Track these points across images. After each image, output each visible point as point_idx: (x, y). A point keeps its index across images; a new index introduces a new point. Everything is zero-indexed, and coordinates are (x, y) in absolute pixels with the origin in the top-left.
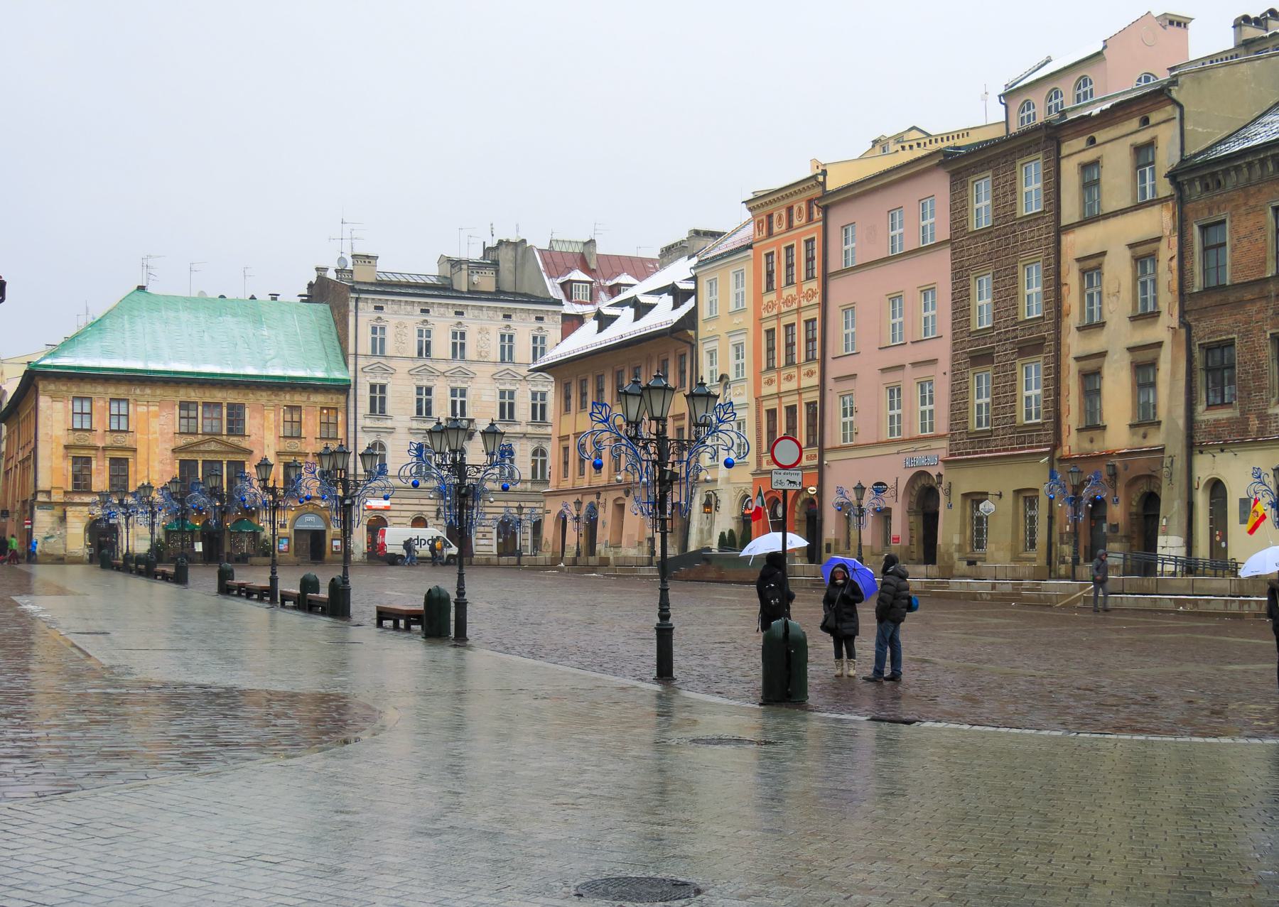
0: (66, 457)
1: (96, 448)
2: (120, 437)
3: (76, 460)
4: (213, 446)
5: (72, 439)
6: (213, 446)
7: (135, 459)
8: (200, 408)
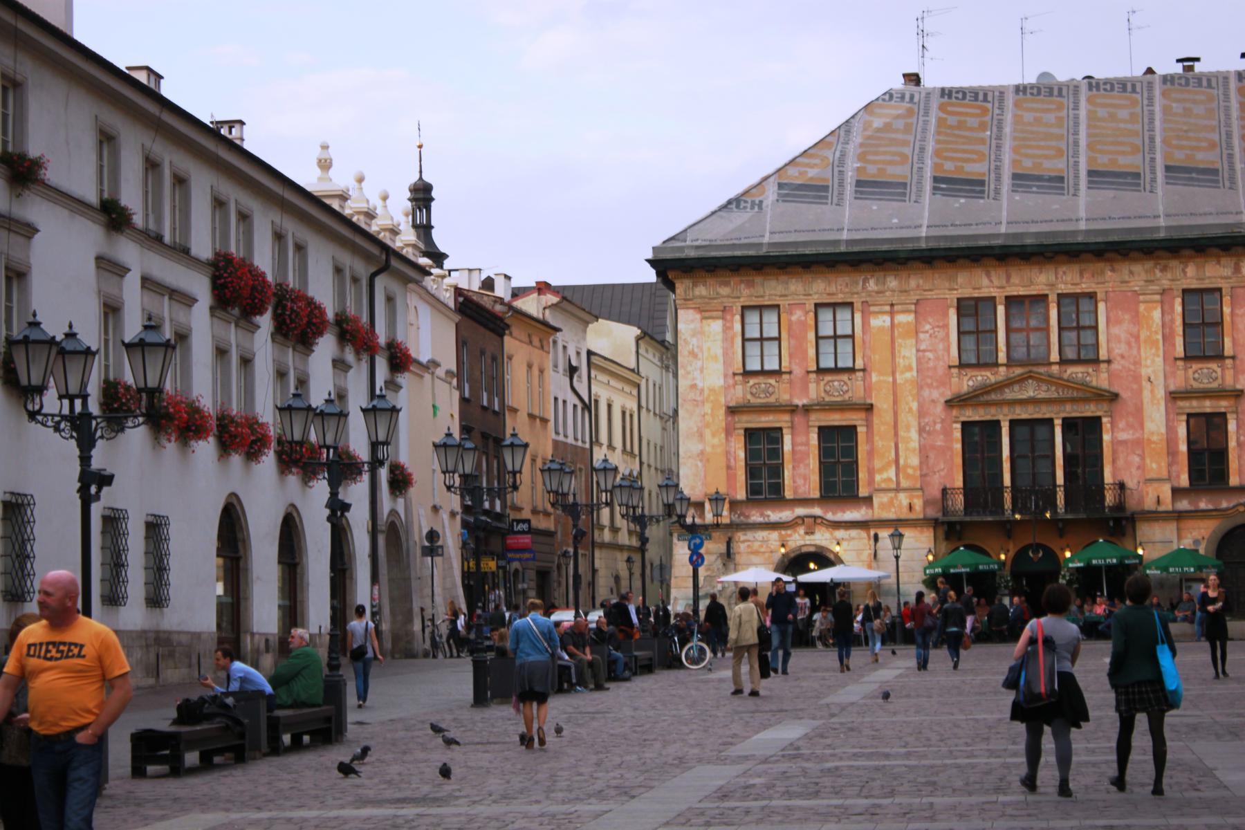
0: (728, 432)
1: (792, 410)
2: (836, 381)
3: (751, 435)
4: (1030, 391)
5: (739, 393)
6: (1030, 391)
7: (869, 425)
8: (1001, 310)
